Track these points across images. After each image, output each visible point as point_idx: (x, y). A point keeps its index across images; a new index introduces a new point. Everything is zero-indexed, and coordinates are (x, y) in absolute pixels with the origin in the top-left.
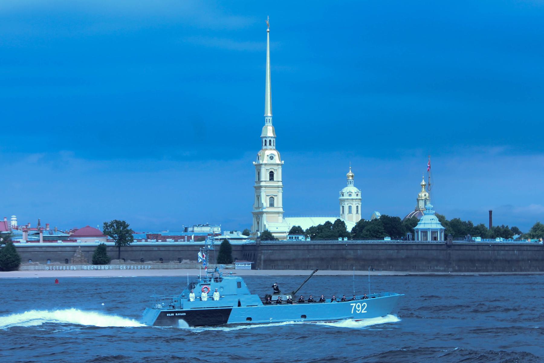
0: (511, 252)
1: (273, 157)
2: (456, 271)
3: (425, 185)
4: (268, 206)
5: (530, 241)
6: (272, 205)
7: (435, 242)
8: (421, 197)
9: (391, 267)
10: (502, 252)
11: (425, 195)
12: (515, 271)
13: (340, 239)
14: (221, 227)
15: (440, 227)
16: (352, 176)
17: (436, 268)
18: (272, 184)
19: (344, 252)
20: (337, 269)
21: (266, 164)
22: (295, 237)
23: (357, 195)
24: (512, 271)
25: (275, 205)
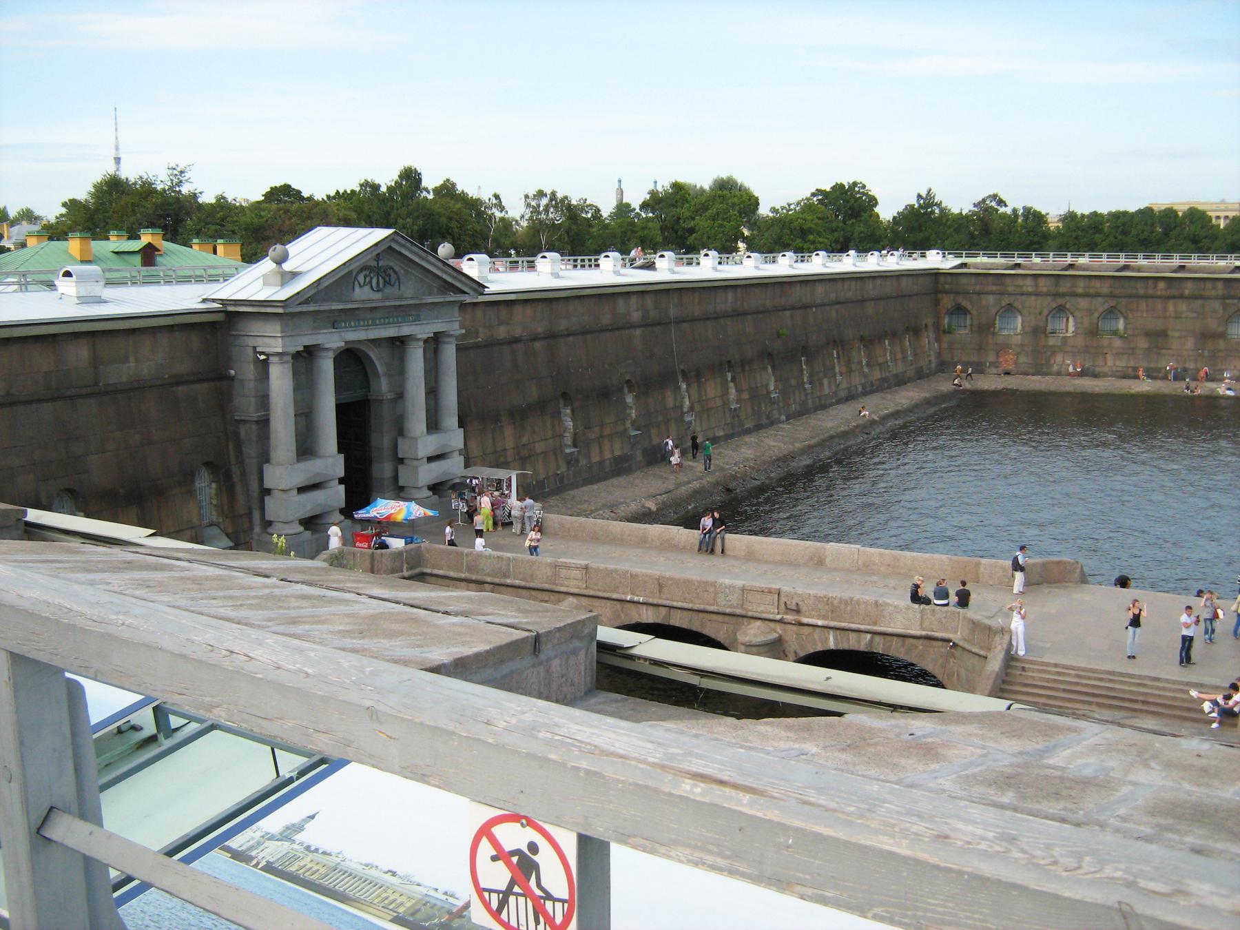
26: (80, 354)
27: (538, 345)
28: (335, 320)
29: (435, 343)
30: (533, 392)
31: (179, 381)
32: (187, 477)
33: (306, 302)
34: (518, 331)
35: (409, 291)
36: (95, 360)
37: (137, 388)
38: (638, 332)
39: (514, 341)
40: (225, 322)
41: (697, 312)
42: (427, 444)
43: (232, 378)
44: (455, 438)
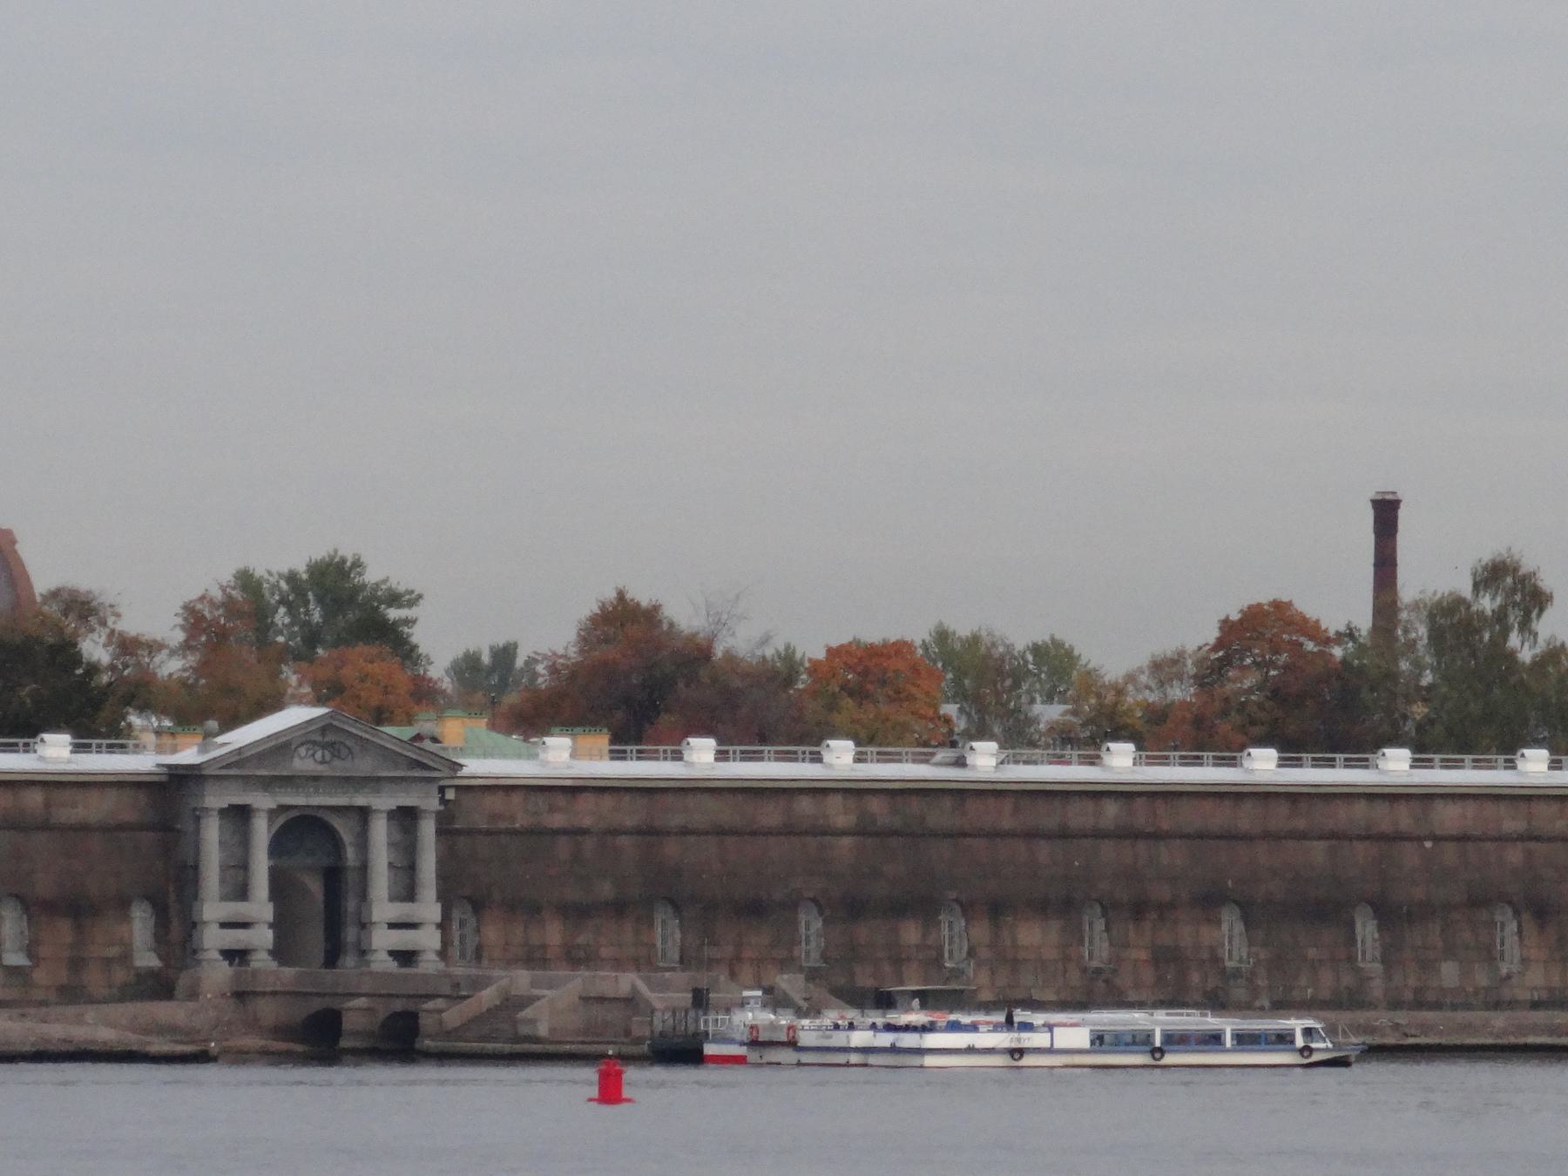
26: (35, 798)
27: (623, 840)
28: (268, 784)
29: (406, 817)
30: (606, 890)
31: (122, 827)
32: (123, 905)
33: (228, 766)
34: (587, 822)
35: (364, 765)
36: (47, 805)
37: (84, 828)
38: (846, 841)
41: (1007, 823)
43: (179, 831)
44: (429, 908)
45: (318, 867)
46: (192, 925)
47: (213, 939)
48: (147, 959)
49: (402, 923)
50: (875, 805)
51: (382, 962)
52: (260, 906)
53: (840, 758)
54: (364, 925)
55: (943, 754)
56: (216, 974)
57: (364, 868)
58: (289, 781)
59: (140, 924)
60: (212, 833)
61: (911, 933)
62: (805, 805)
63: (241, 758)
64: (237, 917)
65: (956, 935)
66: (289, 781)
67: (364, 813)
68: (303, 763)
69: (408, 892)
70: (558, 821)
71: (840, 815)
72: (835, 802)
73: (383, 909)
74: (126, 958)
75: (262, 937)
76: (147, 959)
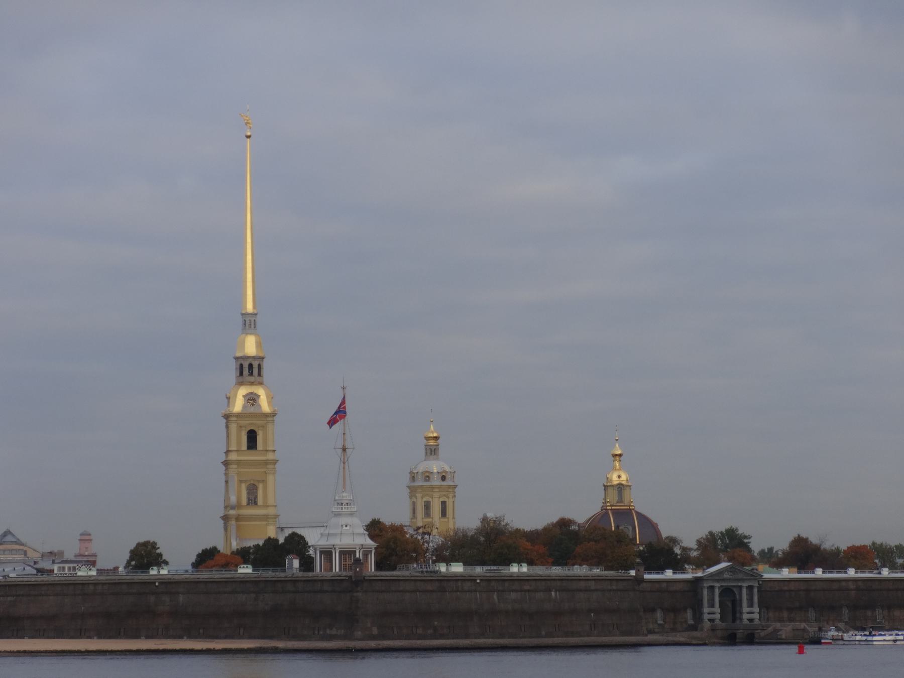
0: (540, 595)
1: (254, 400)
2: (373, 638)
3: (620, 455)
4: (244, 501)
5: (786, 573)
6: (253, 501)
7: (328, 575)
8: (611, 481)
9: (242, 631)
10: (513, 595)
11: (619, 477)
12: (550, 635)
13: (153, 572)
14: (677, 555)
15: (369, 542)
16: (436, 438)
17: (328, 631)
18: (252, 456)
19: (152, 598)
20: (137, 637)
21: (238, 415)
22: (69, 569)
23: (444, 478)
24: (542, 637)
25: (260, 501)
28: (718, 581)
32: (685, 609)
35: (740, 576)
39: (790, 591)
40: (698, 580)
42: (748, 610)
44: (756, 609)
45: (730, 601)
46: (701, 614)
47: (706, 617)
48: (691, 622)
49: (750, 613)
50: (860, 583)
51: (745, 622)
52: (717, 609)
53: (852, 573)
54: (741, 613)
55: (875, 571)
56: (707, 625)
57: (741, 600)
58: (724, 580)
59: (689, 614)
60: (705, 592)
61: (869, 613)
62: (844, 584)
63: (712, 575)
64: (712, 612)
65: (879, 614)
66: (724, 580)
67: (741, 587)
68: (726, 576)
69: (751, 605)
70: (786, 588)
71: (852, 586)
72: (850, 583)
73: (746, 609)
74: (686, 621)
75: (718, 616)
76: (691, 622)
